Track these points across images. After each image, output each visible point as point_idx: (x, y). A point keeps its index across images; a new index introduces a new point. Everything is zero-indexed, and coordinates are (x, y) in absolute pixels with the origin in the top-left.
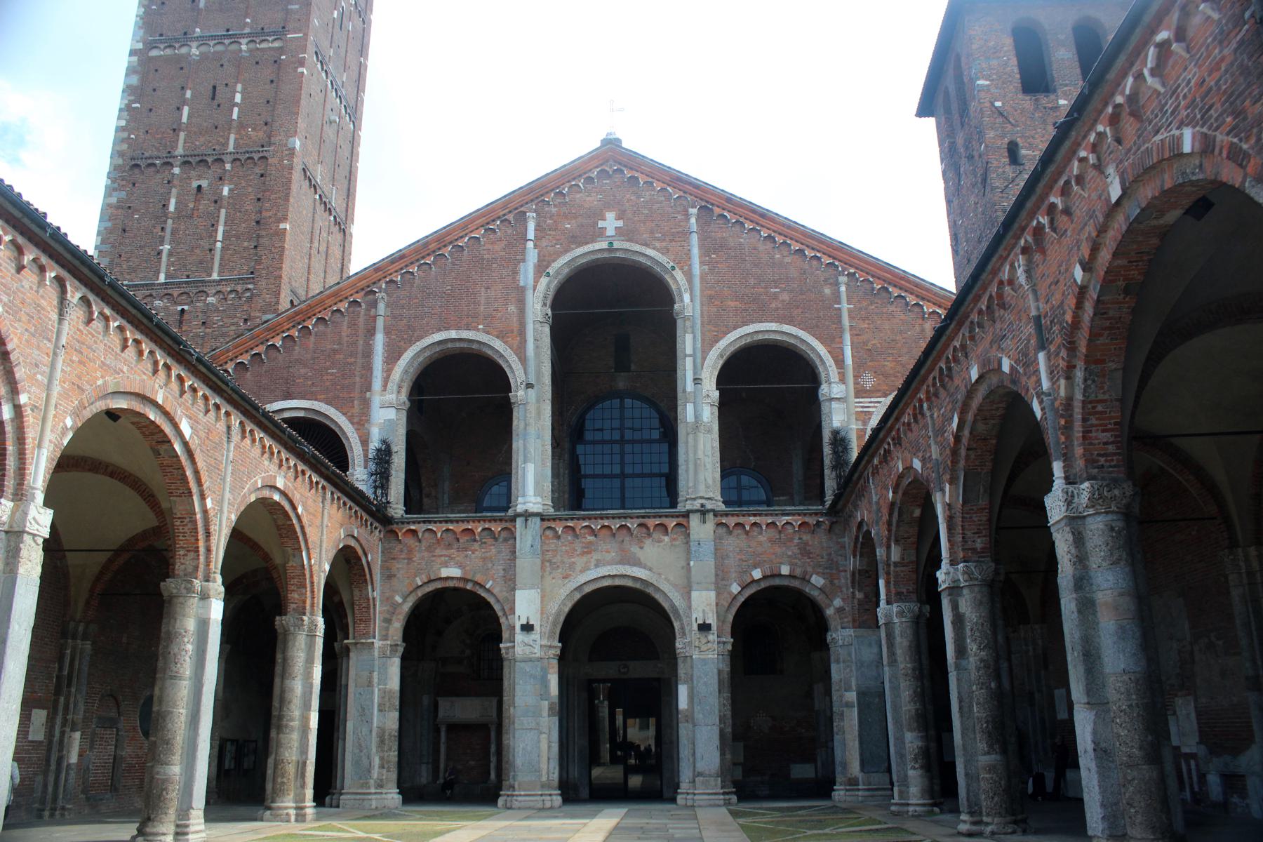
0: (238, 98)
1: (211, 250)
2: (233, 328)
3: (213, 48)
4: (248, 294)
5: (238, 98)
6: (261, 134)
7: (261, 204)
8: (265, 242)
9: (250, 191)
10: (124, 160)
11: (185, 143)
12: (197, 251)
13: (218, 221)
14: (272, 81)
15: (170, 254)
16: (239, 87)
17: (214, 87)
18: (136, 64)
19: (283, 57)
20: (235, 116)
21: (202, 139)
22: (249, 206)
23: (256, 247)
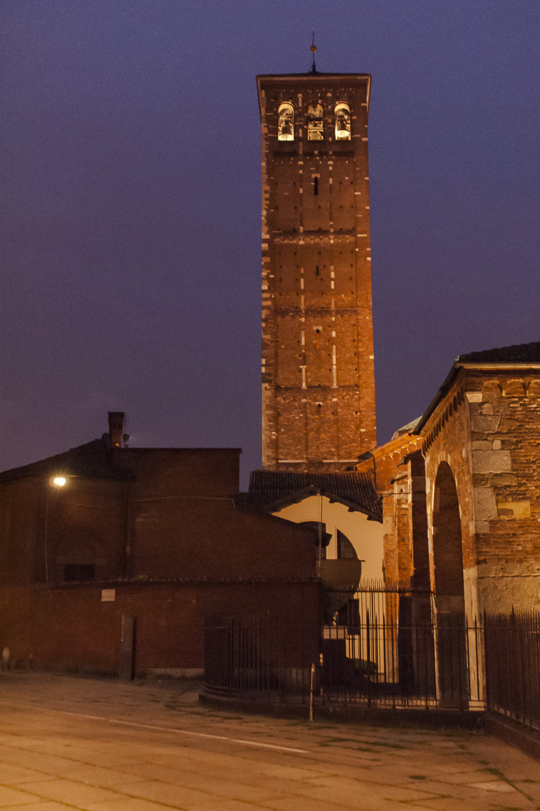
0: (333, 275)
1: (330, 370)
2: (350, 416)
3: (313, 240)
4: (356, 397)
5: (333, 275)
6: (350, 298)
7: (356, 343)
8: (362, 366)
9: (348, 334)
10: (271, 312)
11: (305, 301)
12: (323, 370)
13: (332, 352)
14: (352, 265)
15: (307, 371)
16: (332, 268)
17: (318, 268)
18: (267, 249)
19: (357, 250)
20: (333, 287)
21: (315, 300)
22: (349, 344)
23: (356, 370)
